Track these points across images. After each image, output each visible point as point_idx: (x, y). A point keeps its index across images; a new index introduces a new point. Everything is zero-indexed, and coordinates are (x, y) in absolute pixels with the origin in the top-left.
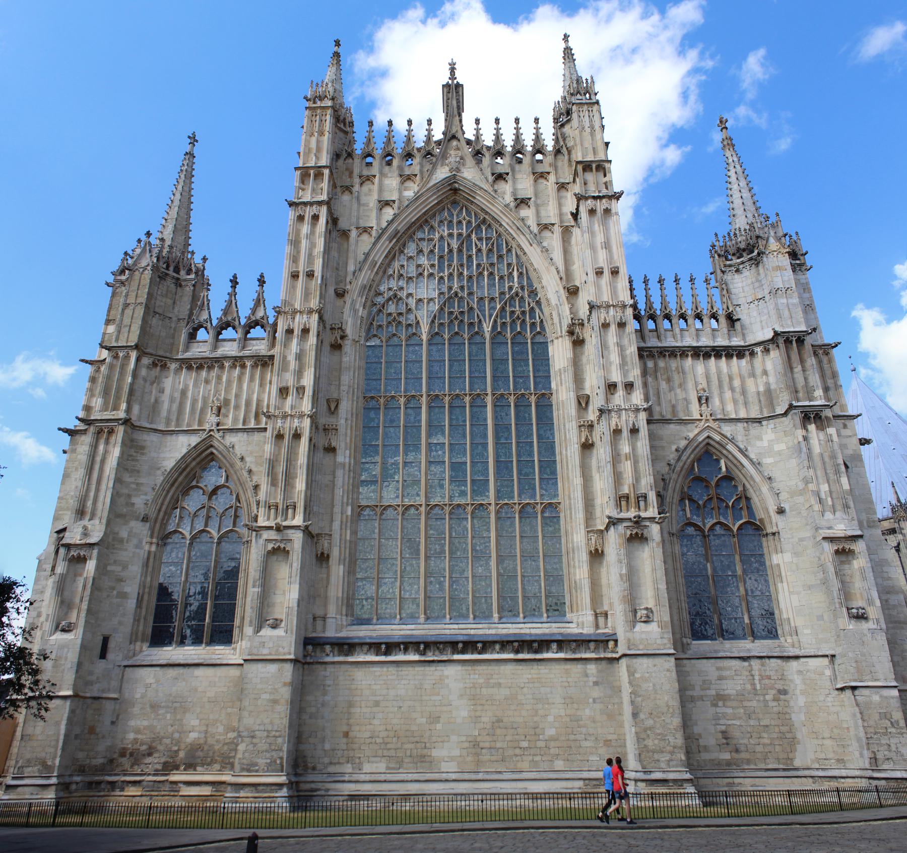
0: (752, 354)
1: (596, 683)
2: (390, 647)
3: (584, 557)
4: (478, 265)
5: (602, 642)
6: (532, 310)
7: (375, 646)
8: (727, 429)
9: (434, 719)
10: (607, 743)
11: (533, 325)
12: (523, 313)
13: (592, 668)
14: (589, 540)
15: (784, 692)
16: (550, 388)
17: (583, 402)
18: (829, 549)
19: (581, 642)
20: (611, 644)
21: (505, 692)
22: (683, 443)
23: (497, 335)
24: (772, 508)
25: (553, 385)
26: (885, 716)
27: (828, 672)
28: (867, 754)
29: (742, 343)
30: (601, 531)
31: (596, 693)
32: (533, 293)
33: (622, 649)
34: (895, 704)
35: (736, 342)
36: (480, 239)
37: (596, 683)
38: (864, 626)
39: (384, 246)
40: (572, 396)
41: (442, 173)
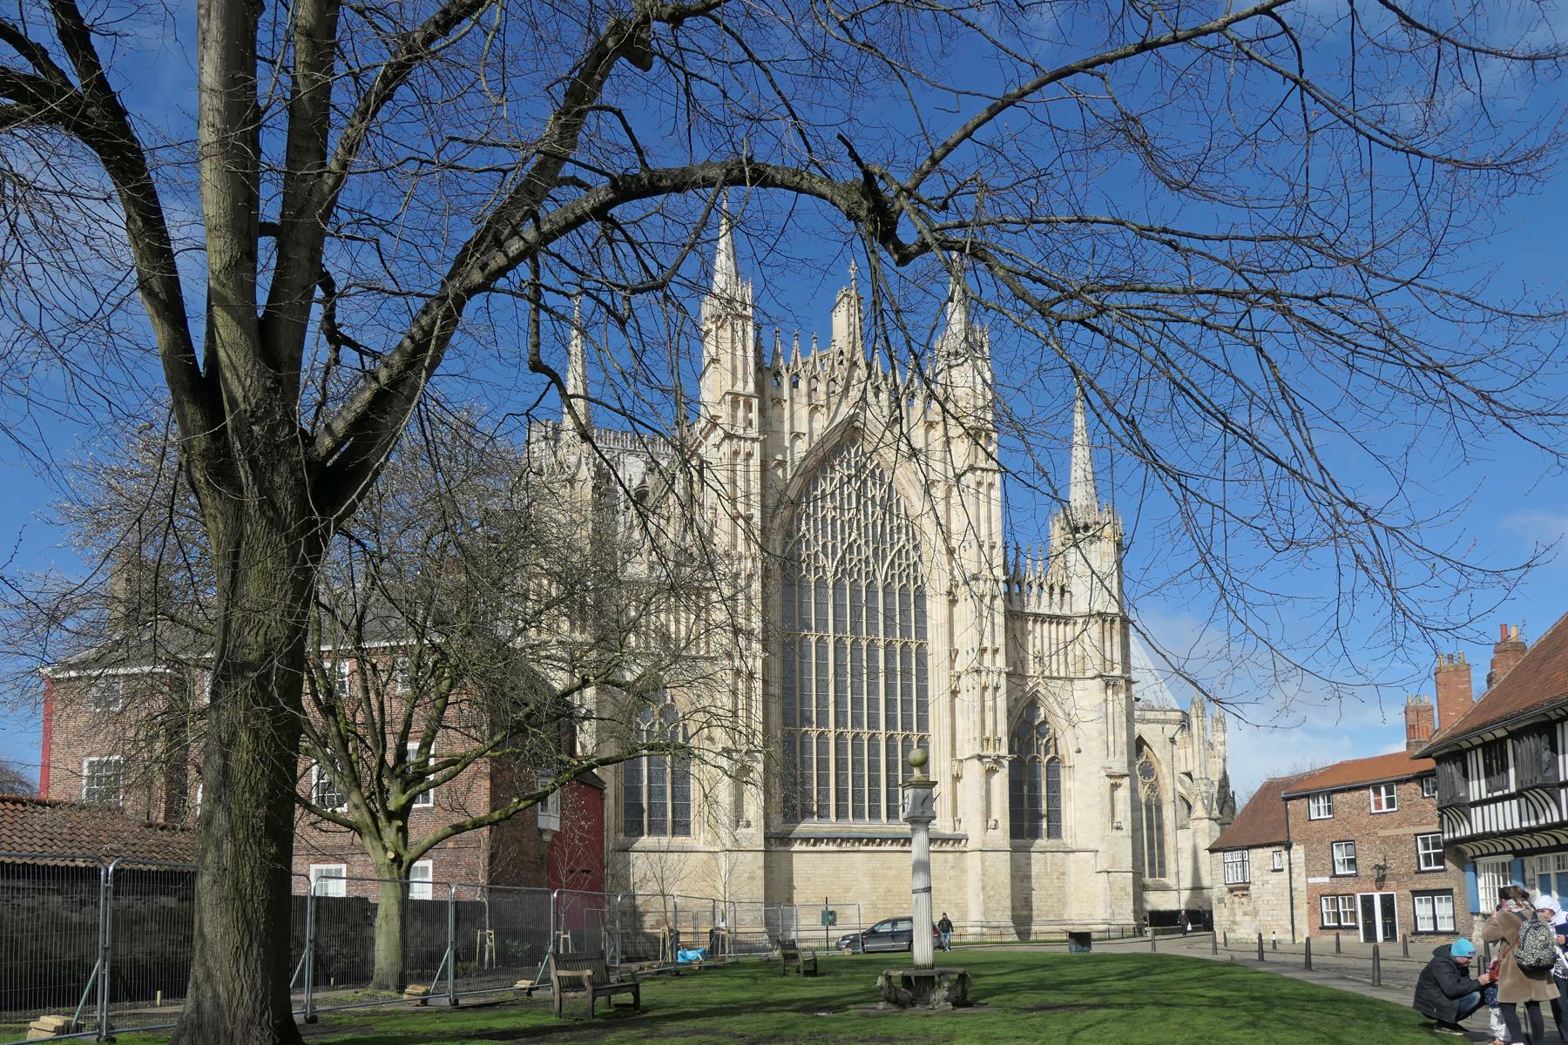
0: (1075, 624)
1: (952, 868)
2: (818, 840)
3: (949, 779)
4: (873, 513)
5: (958, 840)
6: (915, 563)
7: (806, 840)
8: (1052, 683)
9: (847, 890)
10: (957, 905)
11: (916, 578)
12: (908, 566)
13: (950, 856)
14: (952, 766)
15: (1063, 874)
16: (925, 639)
17: (953, 654)
18: (1109, 781)
19: (945, 840)
20: (963, 842)
21: (894, 872)
22: (1020, 694)
23: (887, 588)
24: (1073, 749)
25: (929, 636)
26: (1122, 889)
27: (1092, 862)
28: (1109, 911)
29: (1068, 613)
30: (961, 761)
31: (952, 873)
32: (916, 547)
33: (970, 846)
34: (1130, 881)
35: (1066, 611)
36: (874, 484)
37: (952, 868)
38: (1120, 833)
39: (799, 482)
40: (947, 648)
41: (845, 411)
